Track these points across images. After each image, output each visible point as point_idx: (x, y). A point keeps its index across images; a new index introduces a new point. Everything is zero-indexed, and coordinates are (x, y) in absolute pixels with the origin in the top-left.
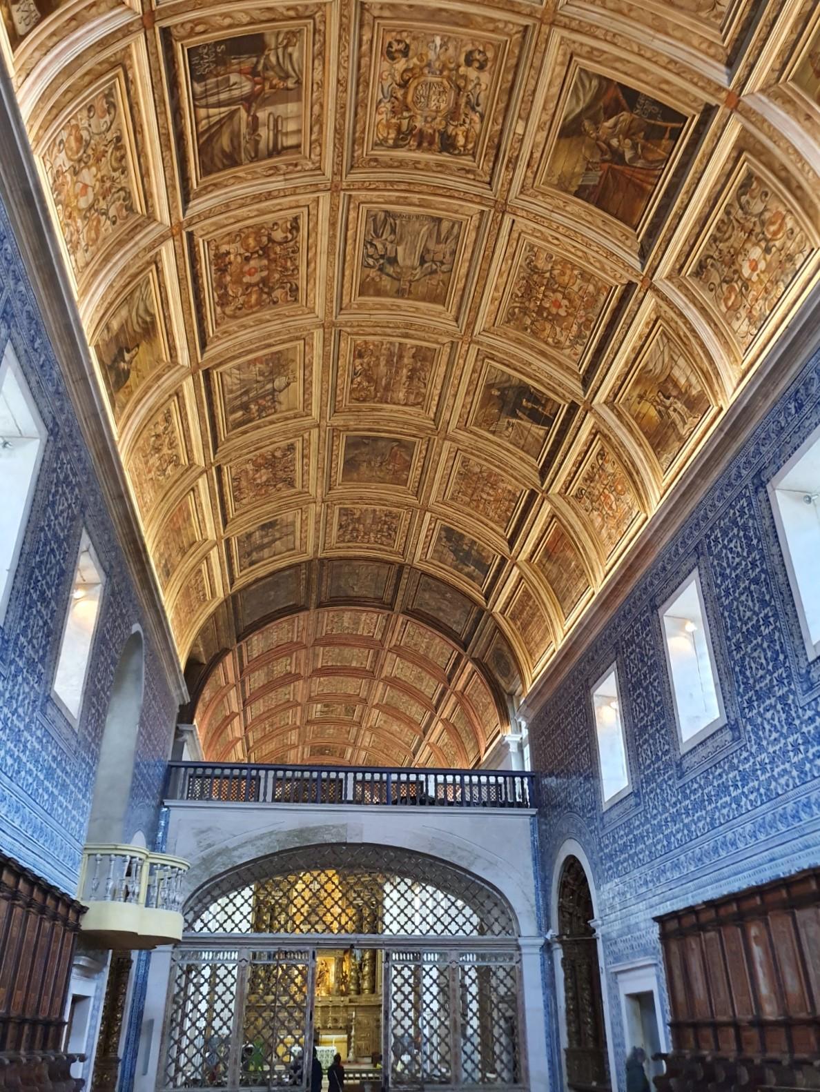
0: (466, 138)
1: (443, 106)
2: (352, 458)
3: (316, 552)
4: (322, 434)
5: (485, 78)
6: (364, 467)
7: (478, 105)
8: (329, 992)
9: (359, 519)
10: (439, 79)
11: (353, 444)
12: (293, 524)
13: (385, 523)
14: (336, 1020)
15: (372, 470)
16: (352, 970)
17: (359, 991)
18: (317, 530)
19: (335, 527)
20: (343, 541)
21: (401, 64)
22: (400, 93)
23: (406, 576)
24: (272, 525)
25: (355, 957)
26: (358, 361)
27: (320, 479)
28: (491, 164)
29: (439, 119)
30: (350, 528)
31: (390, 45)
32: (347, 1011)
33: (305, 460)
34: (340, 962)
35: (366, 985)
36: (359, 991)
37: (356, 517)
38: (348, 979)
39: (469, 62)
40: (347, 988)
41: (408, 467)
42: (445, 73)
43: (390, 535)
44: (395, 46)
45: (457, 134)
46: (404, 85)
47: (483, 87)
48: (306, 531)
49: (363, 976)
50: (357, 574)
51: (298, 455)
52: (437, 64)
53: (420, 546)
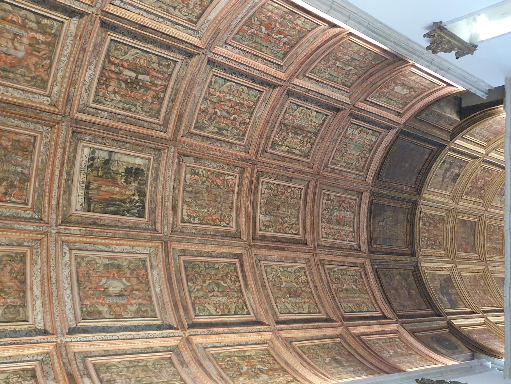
2: (466, 224)
3: (425, 199)
4: (482, 212)
6: (462, 230)
9: (437, 227)
11: (473, 226)
12: (446, 190)
13: (435, 242)
15: (461, 233)
18: (439, 202)
19: (434, 213)
20: (423, 217)
23: (408, 259)
24: (454, 180)
26: (497, 227)
27: (466, 208)
30: (431, 221)
33: (472, 202)
37: (438, 225)
41: (465, 251)
43: (429, 245)
48: (438, 196)
50: (396, 225)
51: (477, 200)
53: (431, 265)
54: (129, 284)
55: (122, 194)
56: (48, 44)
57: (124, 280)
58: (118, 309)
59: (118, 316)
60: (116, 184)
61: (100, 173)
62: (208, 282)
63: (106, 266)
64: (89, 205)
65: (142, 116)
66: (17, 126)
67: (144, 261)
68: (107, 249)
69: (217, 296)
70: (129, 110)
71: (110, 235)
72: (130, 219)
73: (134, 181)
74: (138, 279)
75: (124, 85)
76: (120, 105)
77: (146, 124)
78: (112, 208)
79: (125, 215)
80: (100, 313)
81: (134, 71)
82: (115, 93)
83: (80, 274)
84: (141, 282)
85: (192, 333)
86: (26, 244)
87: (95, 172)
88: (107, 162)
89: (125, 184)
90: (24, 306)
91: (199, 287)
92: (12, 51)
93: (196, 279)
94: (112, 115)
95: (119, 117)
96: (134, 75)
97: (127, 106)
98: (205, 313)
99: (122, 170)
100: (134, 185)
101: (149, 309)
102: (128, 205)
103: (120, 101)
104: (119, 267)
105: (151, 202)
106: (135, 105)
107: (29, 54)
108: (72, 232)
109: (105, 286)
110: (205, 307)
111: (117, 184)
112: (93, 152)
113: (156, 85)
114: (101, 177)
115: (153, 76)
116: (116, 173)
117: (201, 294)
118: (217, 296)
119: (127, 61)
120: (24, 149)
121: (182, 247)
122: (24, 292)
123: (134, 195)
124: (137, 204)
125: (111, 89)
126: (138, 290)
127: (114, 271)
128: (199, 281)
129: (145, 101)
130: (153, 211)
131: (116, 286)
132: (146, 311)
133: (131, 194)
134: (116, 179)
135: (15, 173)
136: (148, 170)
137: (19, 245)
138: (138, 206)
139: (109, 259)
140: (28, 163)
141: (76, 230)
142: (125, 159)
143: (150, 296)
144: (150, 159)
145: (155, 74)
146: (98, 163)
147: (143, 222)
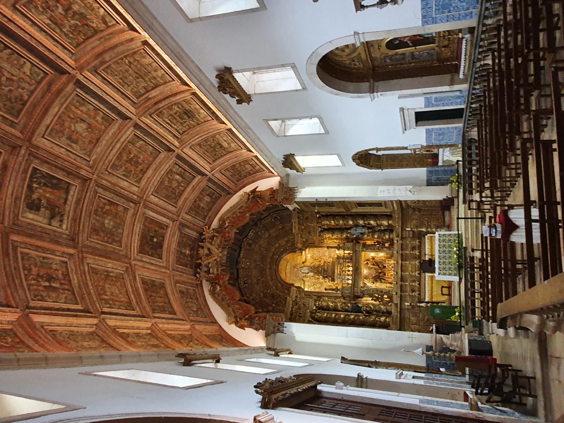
8: (391, 257)
14: (413, 248)
16: (373, 237)
17: (390, 229)
25: (363, 234)
32: (405, 238)
34: (366, 247)
35: (385, 223)
36: (390, 229)
38: (380, 240)
40: (387, 241)
49: (378, 226)
54: (72, 125)
55: (45, 191)
56: (102, 294)
57: (73, 128)
58: (92, 114)
59: (97, 109)
60: (48, 200)
61: (57, 209)
62: (7, 89)
63: (76, 143)
64: (68, 187)
65: (33, 253)
66: (98, 244)
67: (50, 134)
68: (70, 153)
69: (9, 72)
70: (44, 258)
71: (67, 163)
72: (44, 169)
73: (34, 200)
74: (63, 125)
75: (54, 276)
76: (50, 261)
77: (29, 247)
78: (55, 181)
79: (47, 173)
80: (103, 118)
81: (53, 287)
82: (56, 270)
83: (93, 145)
84: (63, 120)
85: (71, 69)
86: (107, 173)
87: (60, 211)
88: (52, 217)
89: (42, 198)
90: (129, 142)
91: (20, 90)
92: (110, 286)
93: (16, 98)
94: (53, 252)
95: (48, 252)
96: (53, 285)
97: (45, 261)
98: (37, 70)
99: (43, 210)
100: (35, 196)
101: (75, 101)
102: (43, 181)
103: (51, 264)
104: (69, 138)
105: (25, 180)
106: (41, 262)
107: (104, 287)
108: (87, 173)
109: (86, 131)
110: (31, 73)
111: (47, 200)
112: (61, 226)
113: (34, 279)
114: (57, 207)
115: (40, 286)
116: (46, 208)
117: (23, 85)
118: (9, 72)
119: (62, 294)
120: (95, 230)
121: (13, 131)
122: (123, 149)
123: (36, 188)
124: (35, 180)
125: (60, 272)
126: (69, 117)
127: (74, 137)
128: (16, 93)
129: (36, 265)
130: (25, 171)
131: (81, 127)
132: (78, 101)
133: (38, 190)
134: (47, 203)
135: (99, 216)
136: (23, 208)
137: (110, 173)
138: (35, 178)
139: (71, 146)
140: (94, 221)
141: (83, 173)
142: (40, 219)
143: (66, 108)
144: (22, 217)
145: (40, 288)
146: (58, 218)
147: (36, 164)
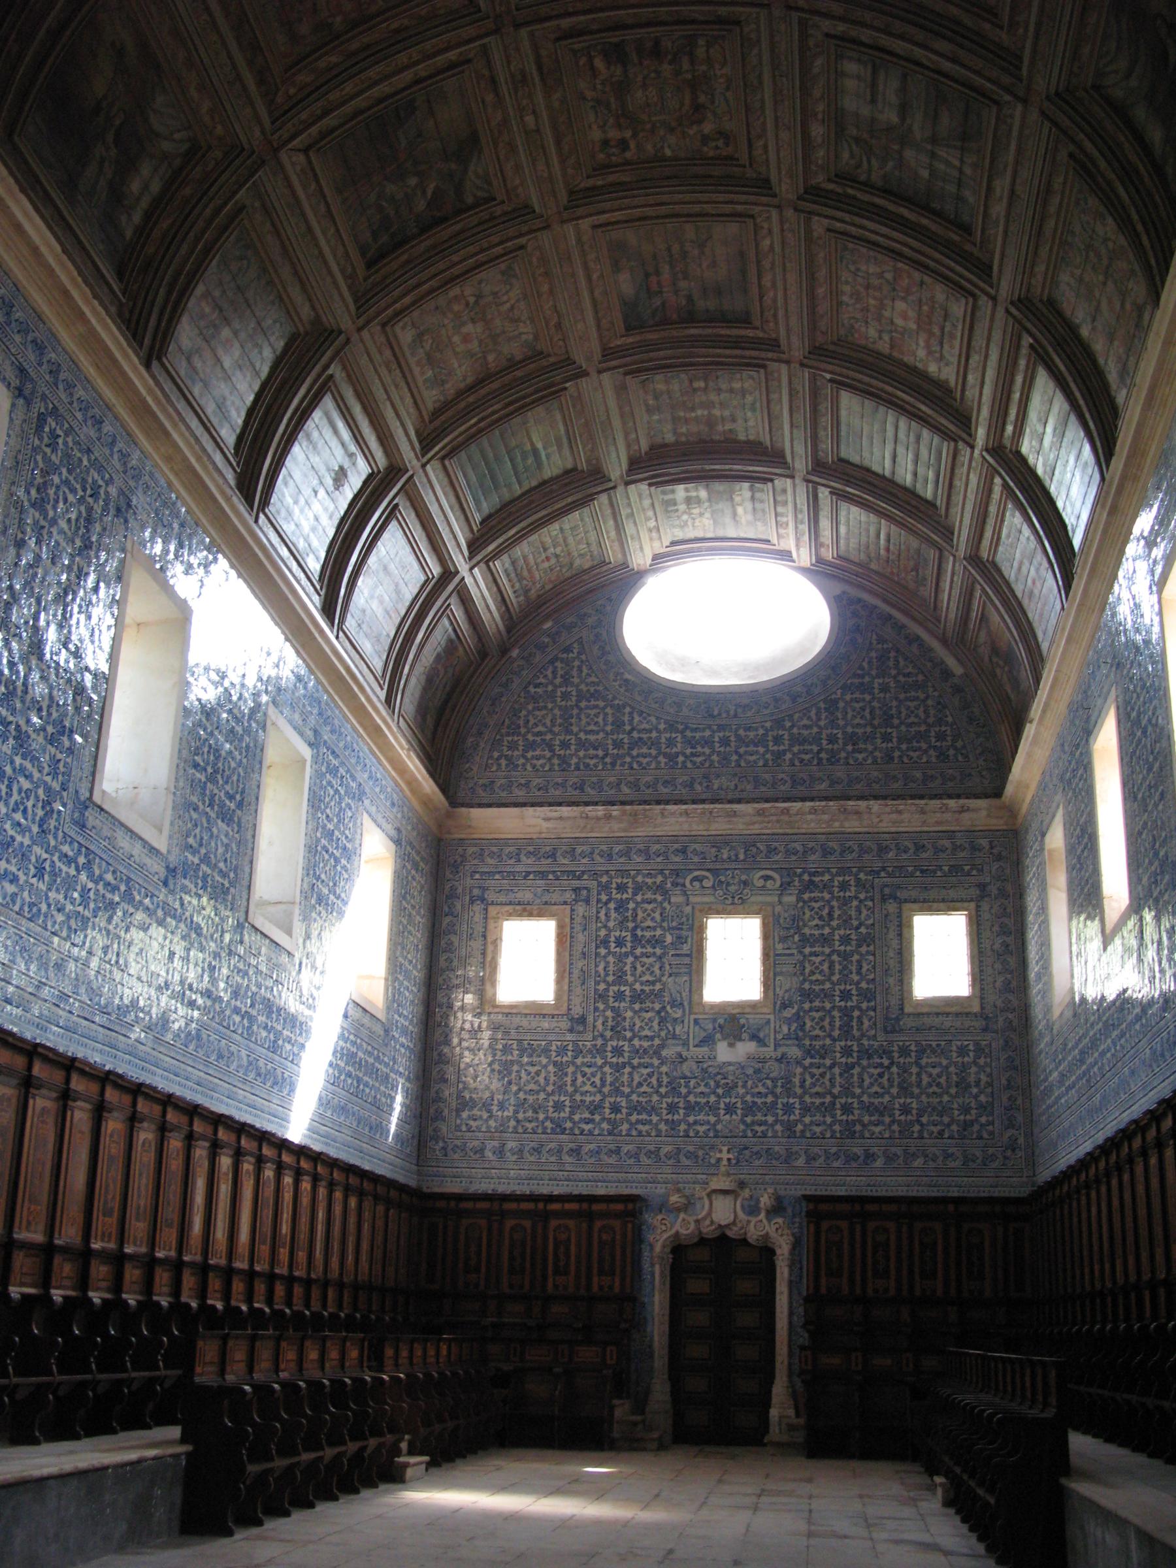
0: (592, 68)
1: (639, 94)
5: (596, 135)
7: (593, 107)
10: (654, 119)
21: (708, 128)
22: (702, 99)
28: (544, 53)
29: (640, 78)
31: (727, 145)
39: (623, 144)
42: (648, 126)
44: (720, 143)
45: (608, 68)
46: (697, 108)
47: (595, 127)
52: (662, 133)
